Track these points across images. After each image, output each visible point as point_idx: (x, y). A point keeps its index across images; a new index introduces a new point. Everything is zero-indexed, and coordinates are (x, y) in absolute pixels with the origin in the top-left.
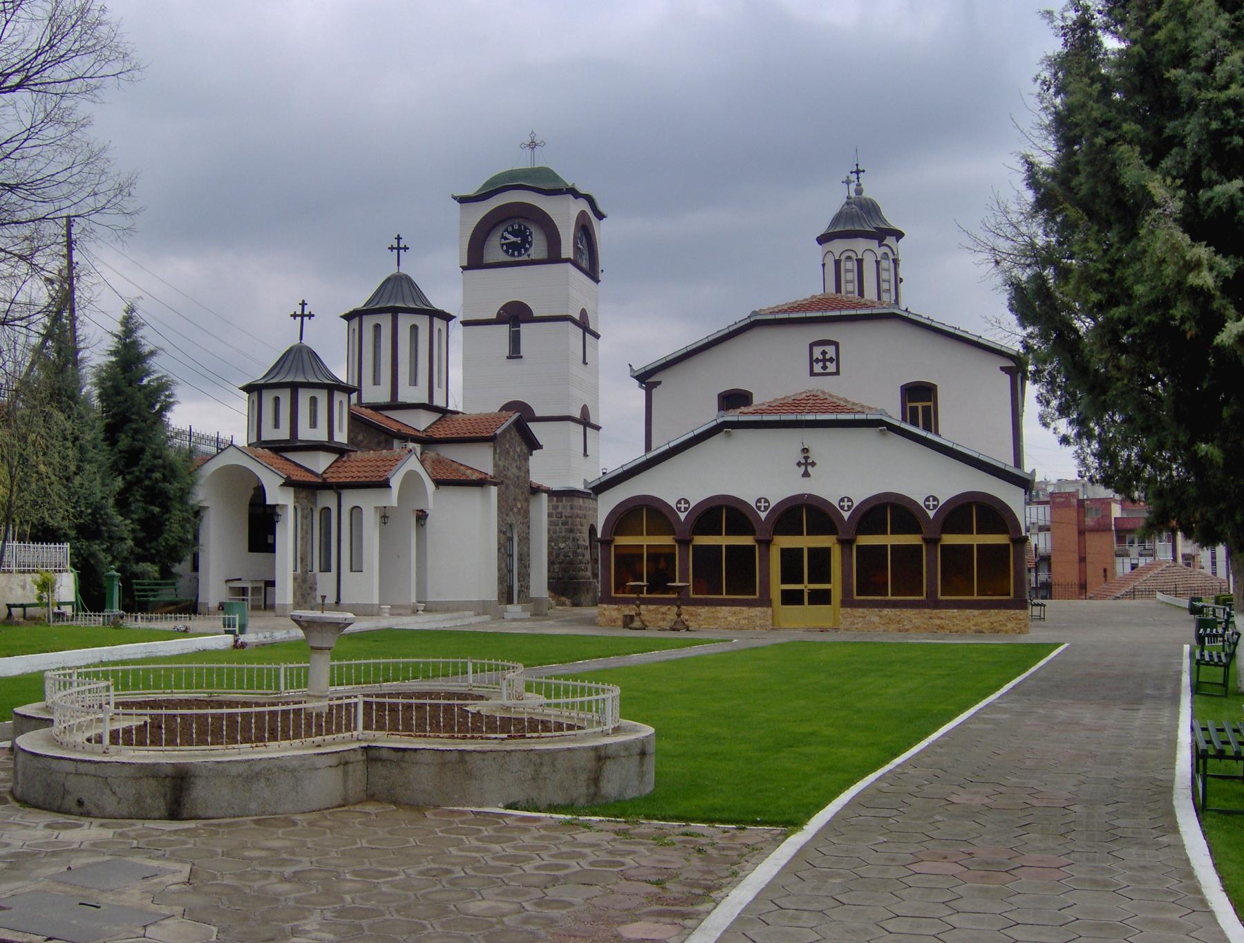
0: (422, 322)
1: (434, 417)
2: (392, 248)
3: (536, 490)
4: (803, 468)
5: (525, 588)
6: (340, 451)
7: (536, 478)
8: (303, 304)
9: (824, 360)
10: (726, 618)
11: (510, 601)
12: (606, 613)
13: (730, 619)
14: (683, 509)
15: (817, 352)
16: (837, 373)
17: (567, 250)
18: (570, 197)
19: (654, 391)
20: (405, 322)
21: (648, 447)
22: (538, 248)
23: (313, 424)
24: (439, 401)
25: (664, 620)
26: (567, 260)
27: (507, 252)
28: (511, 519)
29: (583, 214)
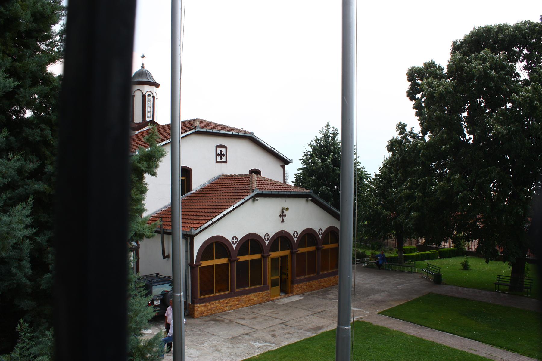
4: (282, 218)
9: (221, 155)
10: (253, 299)
12: (199, 309)
13: (255, 299)
14: (234, 243)
16: (226, 162)
25: (227, 307)
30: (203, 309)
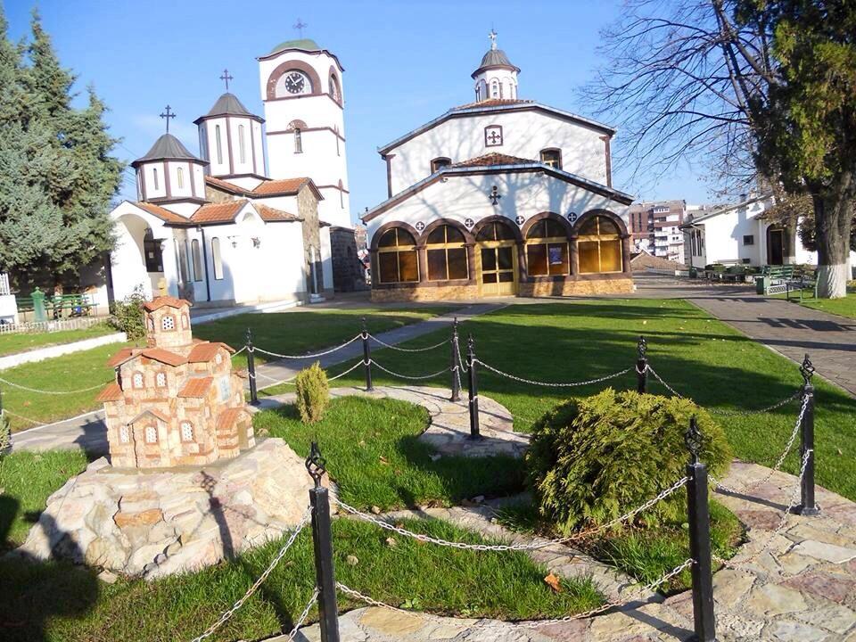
0: (246, 122)
1: (258, 182)
2: (222, 78)
3: (322, 224)
5: (320, 283)
6: (201, 202)
7: (322, 218)
8: (168, 108)
11: (313, 292)
15: (490, 132)
16: (502, 144)
17: (325, 88)
18: (324, 56)
19: (392, 160)
20: (234, 121)
21: (390, 195)
22: (307, 89)
23: (181, 186)
24: (260, 173)
26: (324, 94)
27: (289, 91)
28: (311, 242)
29: (332, 67)
30: (382, 294)
